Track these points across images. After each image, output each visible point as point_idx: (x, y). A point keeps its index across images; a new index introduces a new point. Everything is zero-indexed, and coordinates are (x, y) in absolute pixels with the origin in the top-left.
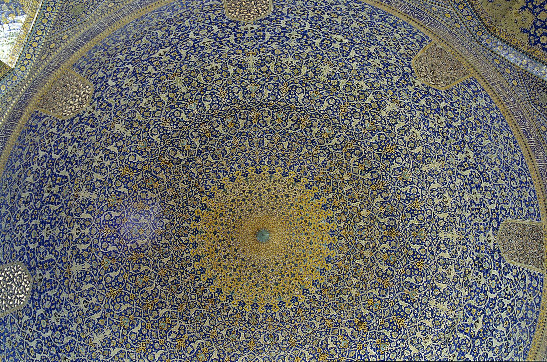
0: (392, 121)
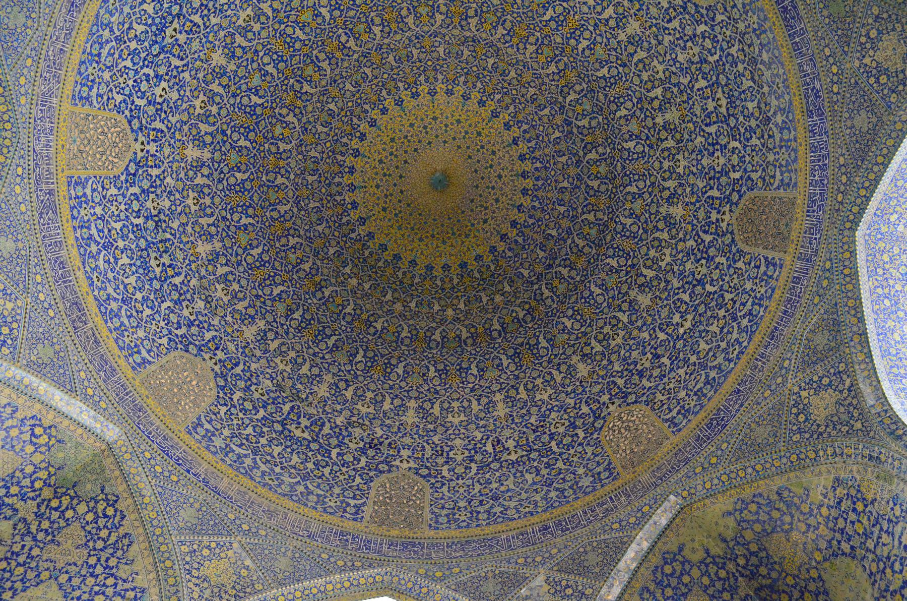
0: (563, 368)
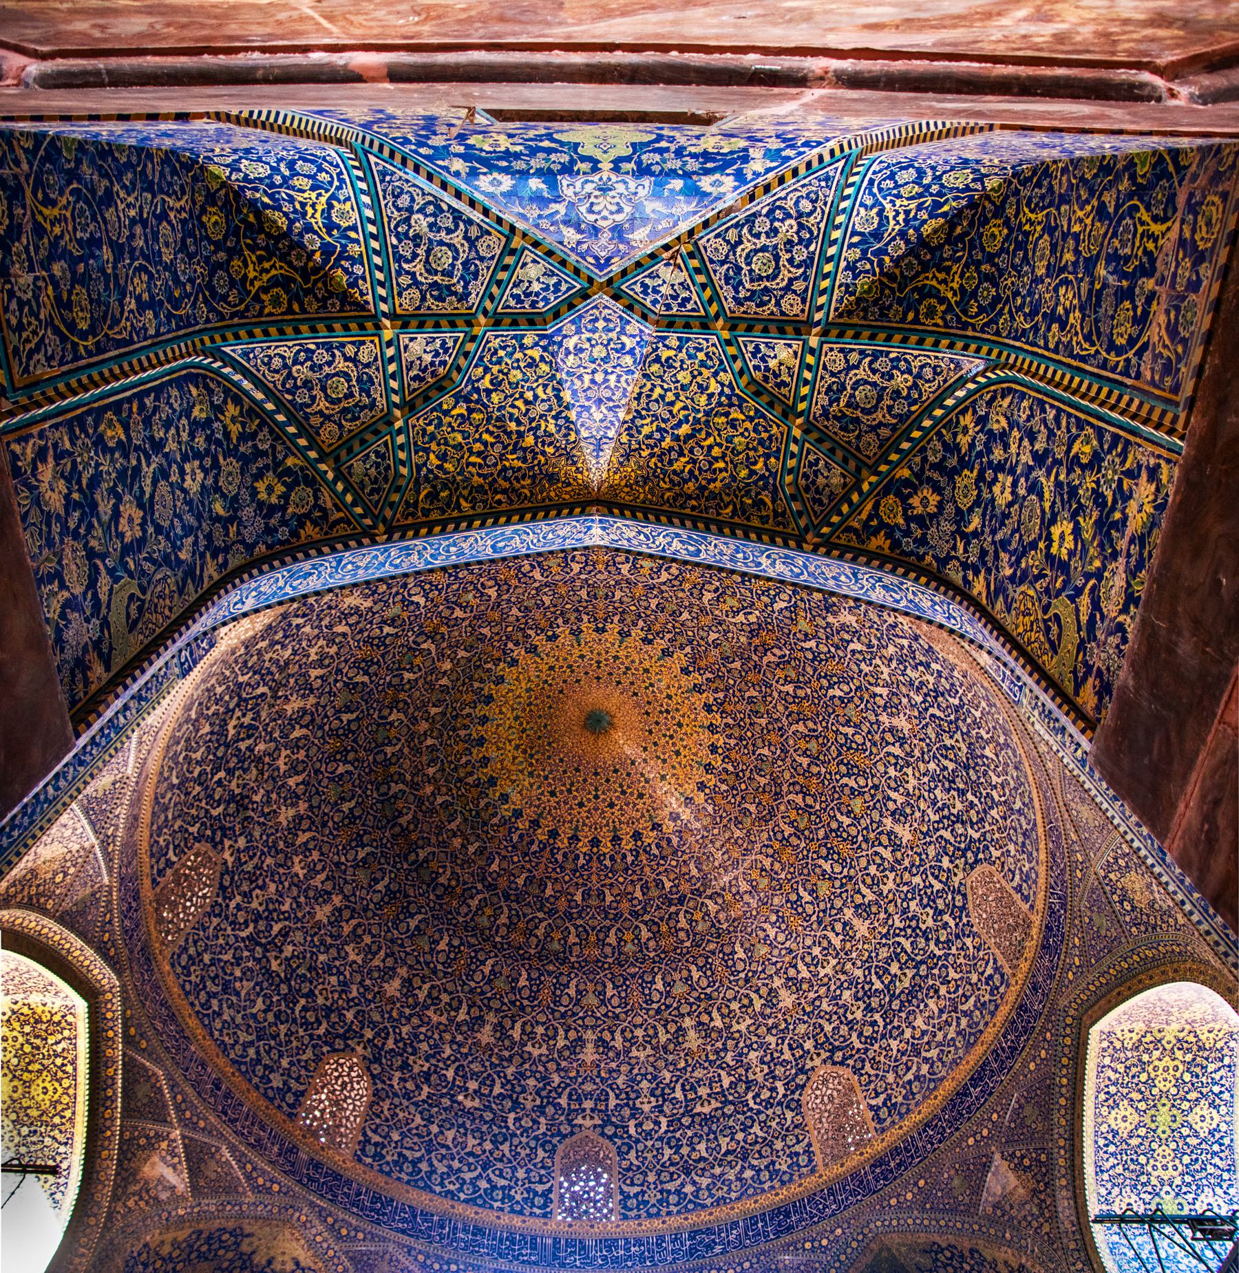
0: (390, 962)
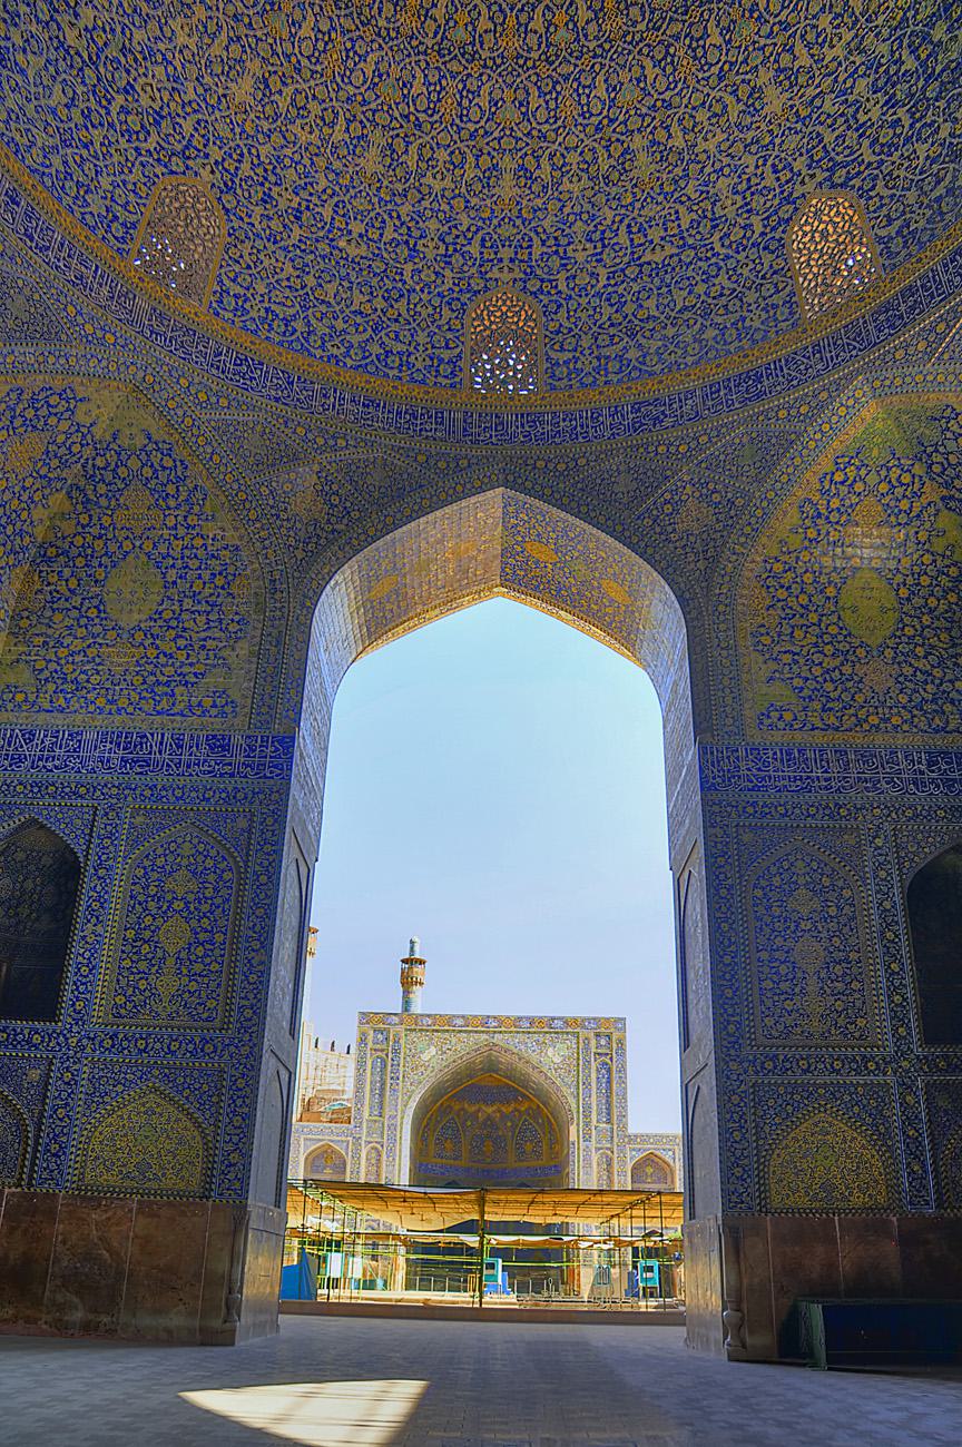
0: (235, 49)
